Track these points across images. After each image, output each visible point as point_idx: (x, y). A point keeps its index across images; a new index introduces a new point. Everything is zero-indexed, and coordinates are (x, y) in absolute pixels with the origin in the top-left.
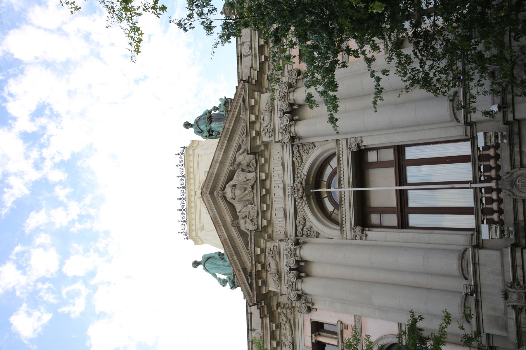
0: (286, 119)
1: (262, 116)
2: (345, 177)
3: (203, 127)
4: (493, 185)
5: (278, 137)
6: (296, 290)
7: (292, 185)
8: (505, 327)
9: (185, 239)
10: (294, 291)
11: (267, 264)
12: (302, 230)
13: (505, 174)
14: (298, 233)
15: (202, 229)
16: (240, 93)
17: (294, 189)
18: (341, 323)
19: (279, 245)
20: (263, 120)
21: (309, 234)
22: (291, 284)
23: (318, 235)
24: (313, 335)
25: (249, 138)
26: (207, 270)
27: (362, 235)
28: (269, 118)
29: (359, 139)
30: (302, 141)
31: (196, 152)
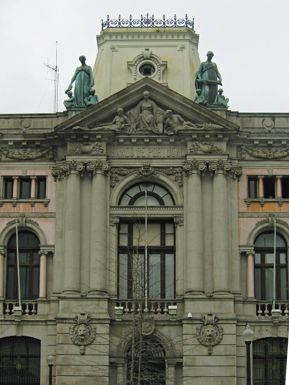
0: (202, 167)
1: (208, 143)
2: (155, 211)
3: (206, 74)
5: (190, 158)
6: (70, 169)
7: (151, 166)
8: (64, 311)
9: (102, 20)
10: (69, 167)
11: (88, 143)
12: (116, 173)
14: (113, 169)
15: (113, 49)
17: (147, 168)
18: (49, 202)
19: (104, 155)
20: (205, 144)
21: (112, 179)
22: (75, 165)
23: (112, 187)
24: (35, 177)
25: (190, 132)
26: (78, 73)
27: (113, 223)
29: (182, 224)
30: (185, 178)
31: (187, 44)
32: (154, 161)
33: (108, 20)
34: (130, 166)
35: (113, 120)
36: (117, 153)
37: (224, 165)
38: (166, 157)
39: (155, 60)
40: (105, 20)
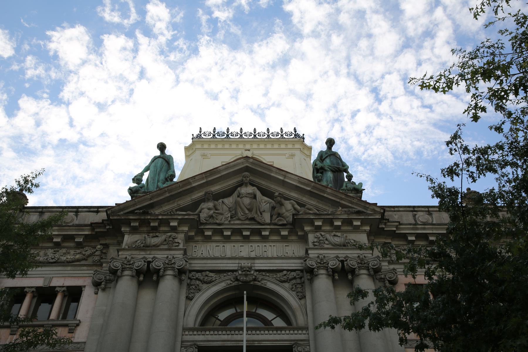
2: (260, 336)
3: (328, 161)
5: (313, 253)
6: (122, 268)
7: (253, 268)
9: (193, 135)
10: (122, 266)
11: (157, 234)
12: (197, 279)
14: (193, 273)
15: (204, 156)
16: (368, 208)
17: (248, 271)
18: (78, 325)
19: (180, 249)
20: (335, 235)
21: (191, 287)
22: (131, 263)
23: (189, 298)
25: (312, 217)
26: (153, 161)
28: (338, 243)
30: (307, 283)
31: (298, 153)
32: (257, 261)
33: (200, 132)
34: (219, 268)
35: (198, 209)
36: (201, 252)
37: (368, 261)
40: (196, 133)
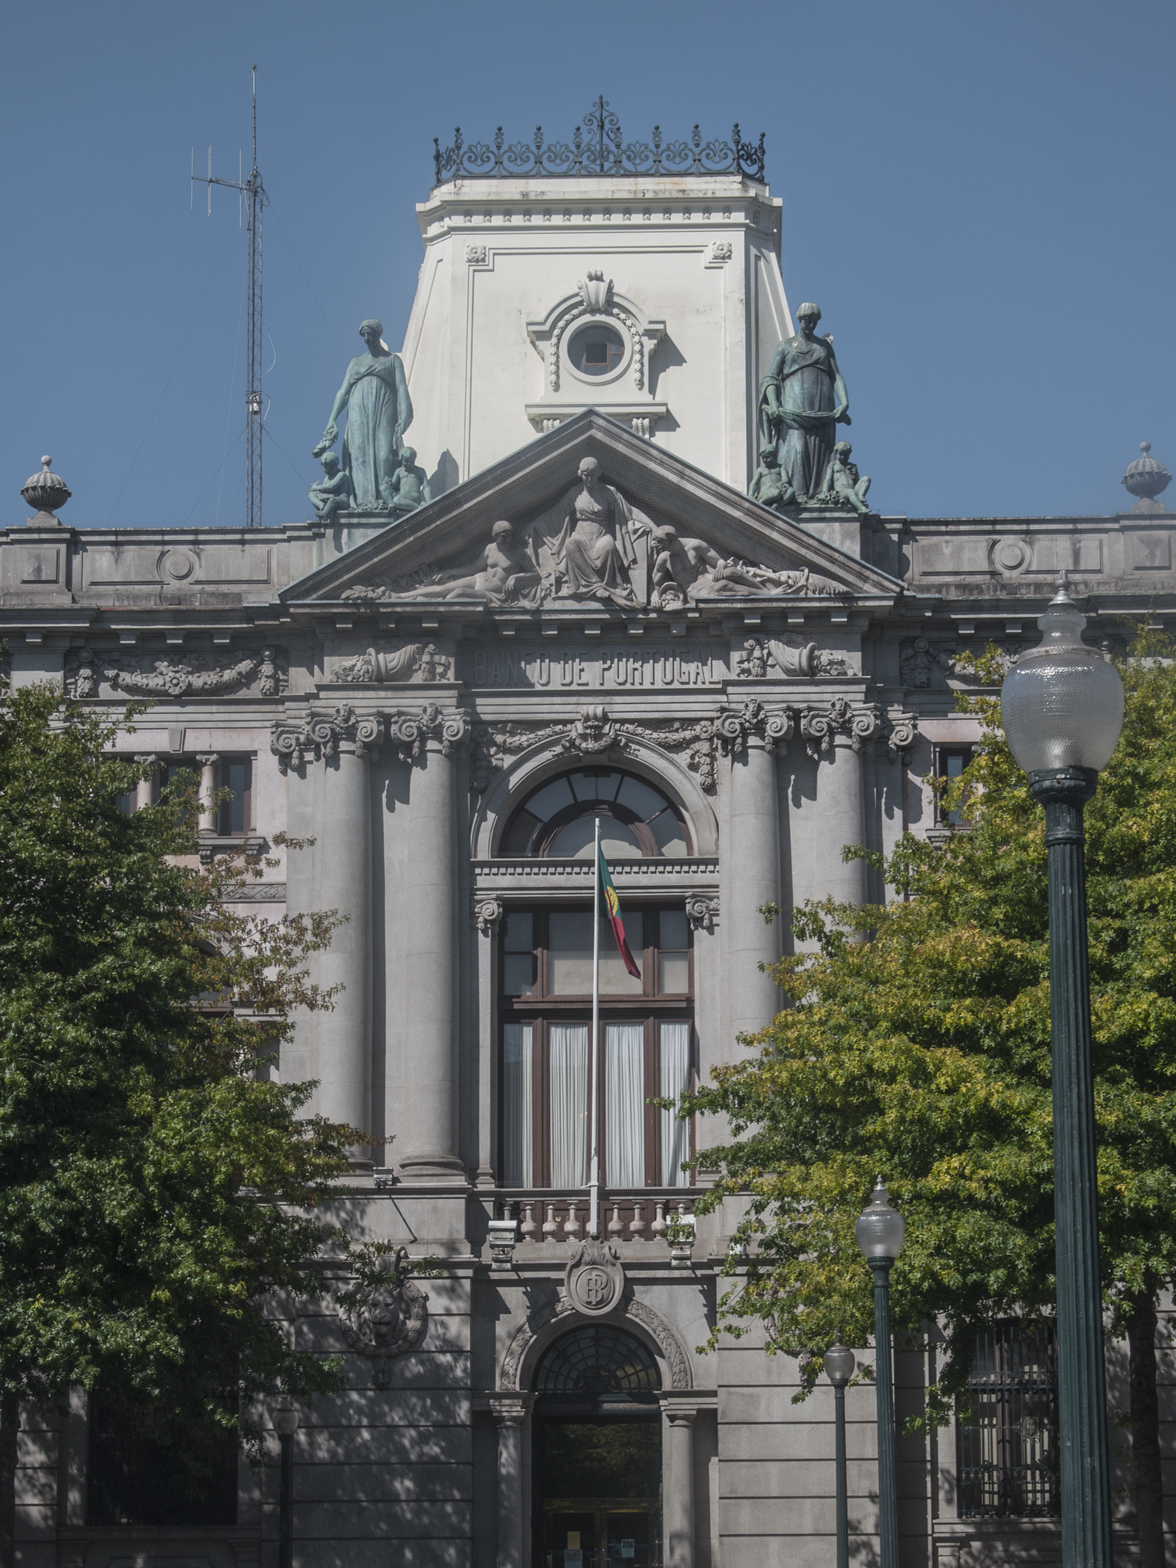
4: (592, 1227)
9: (436, 141)
13: (613, 1251)
24: (214, 757)
38: (659, 685)
39: (623, 316)
